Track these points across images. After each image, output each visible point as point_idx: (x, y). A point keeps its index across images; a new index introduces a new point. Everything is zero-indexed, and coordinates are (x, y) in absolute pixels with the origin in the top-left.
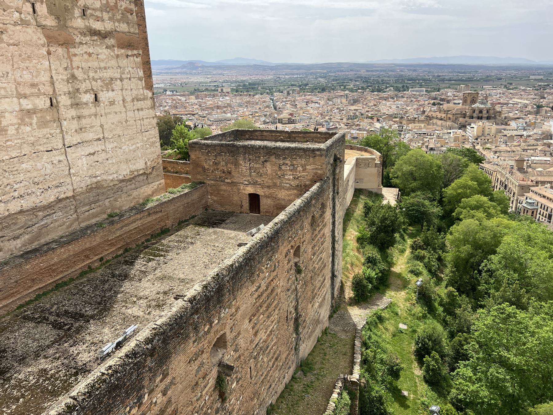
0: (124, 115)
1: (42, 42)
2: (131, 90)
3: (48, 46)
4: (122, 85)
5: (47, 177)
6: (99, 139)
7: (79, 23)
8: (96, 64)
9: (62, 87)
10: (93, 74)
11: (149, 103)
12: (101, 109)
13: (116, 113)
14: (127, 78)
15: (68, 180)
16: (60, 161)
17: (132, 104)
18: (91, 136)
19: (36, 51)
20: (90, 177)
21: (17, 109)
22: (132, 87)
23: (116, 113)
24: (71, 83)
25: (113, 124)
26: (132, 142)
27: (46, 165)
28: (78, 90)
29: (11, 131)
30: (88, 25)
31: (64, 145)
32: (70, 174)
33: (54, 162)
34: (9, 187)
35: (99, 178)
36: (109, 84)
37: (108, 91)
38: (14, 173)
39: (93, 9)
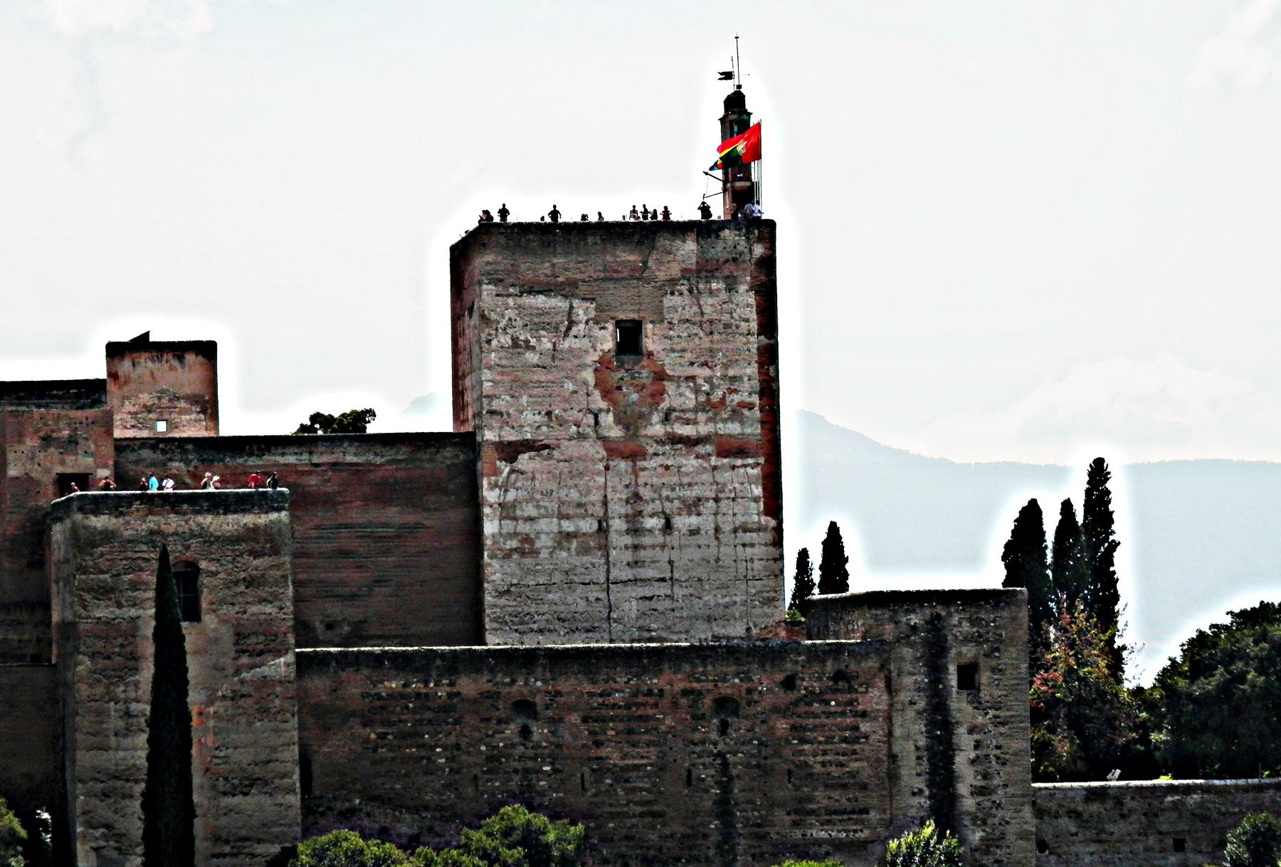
0: (713, 551)
1: (600, 456)
2: (734, 515)
3: (608, 460)
4: (718, 507)
5: (576, 615)
6: (663, 580)
7: (657, 429)
8: (675, 479)
9: (618, 509)
10: (669, 493)
11: (768, 536)
12: (673, 540)
13: (699, 547)
14: (728, 498)
15: (605, 626)
16: (598, 599)
17: (733, 535)
18: (649, 573)
19: (591, 466)
20: (640, 628)
21: (556, 529)
22: (736, 511)
23: (699, 547)
24: (631, 504)
25: (691, 561)
26: (724, 592)
27: (579, 600)
28: (640, 513)
29: (544, 554)
30: (671, 430)
31: (608, 579)
32: (609, 618)
33: (590, 599)
34: (528, 617)
35: (654, 634)
36: (693, 506)
37: (689, 514)
38: (538, 602)
39: (683, 411)
